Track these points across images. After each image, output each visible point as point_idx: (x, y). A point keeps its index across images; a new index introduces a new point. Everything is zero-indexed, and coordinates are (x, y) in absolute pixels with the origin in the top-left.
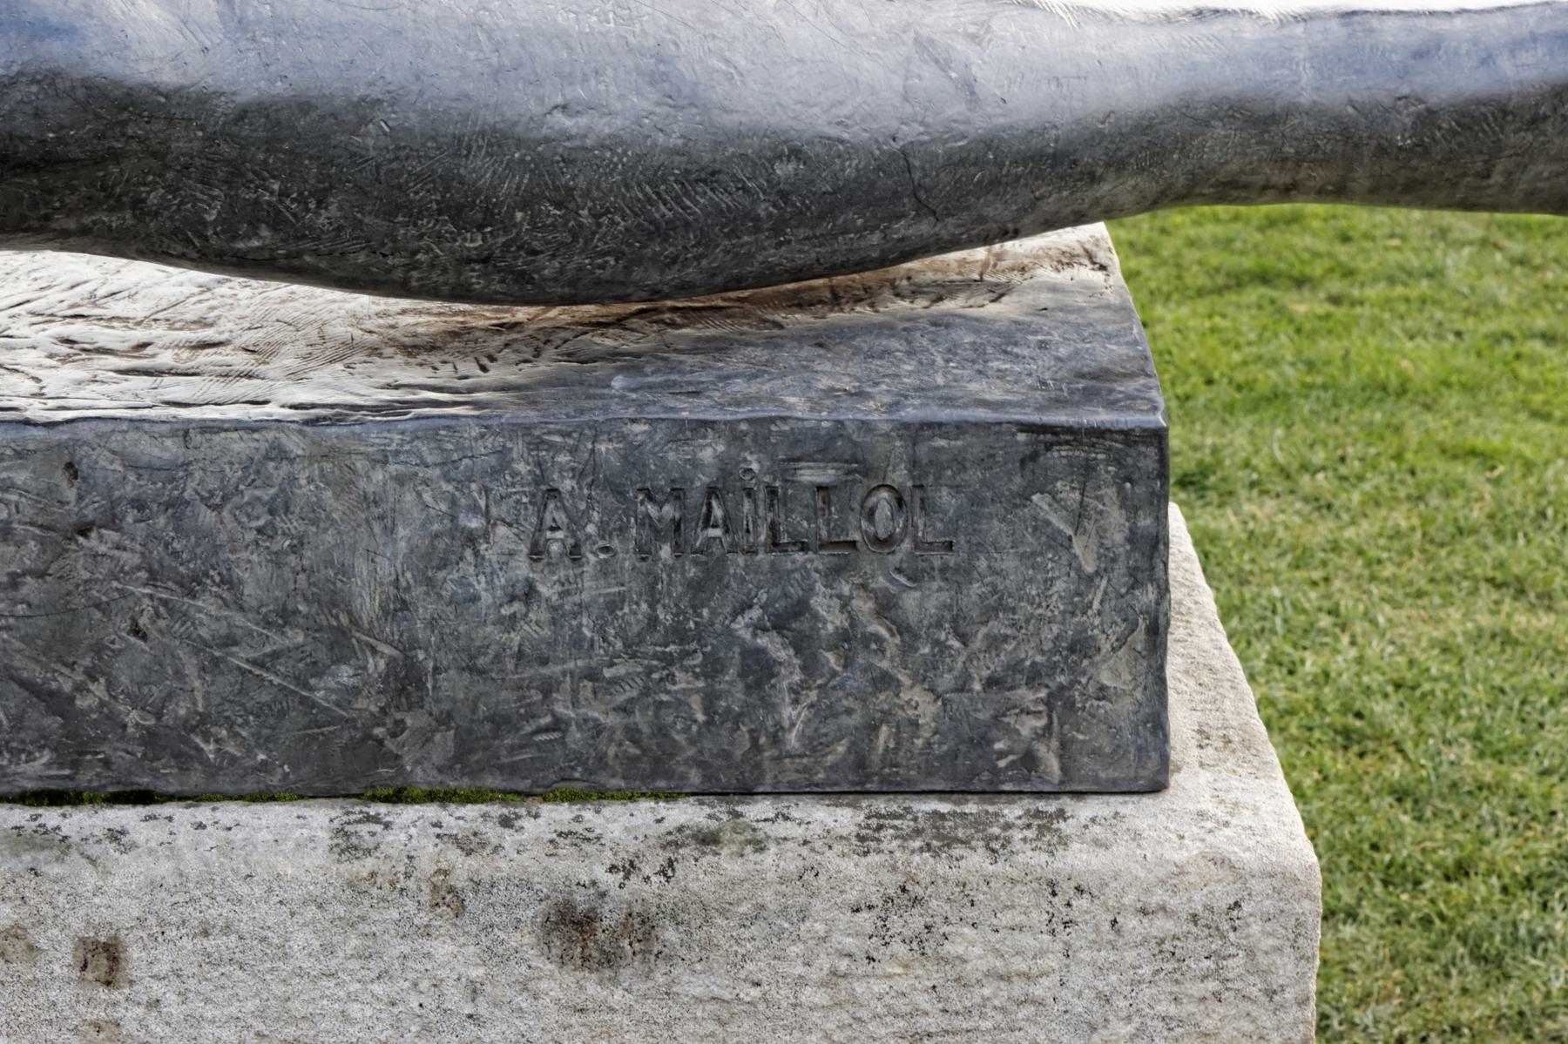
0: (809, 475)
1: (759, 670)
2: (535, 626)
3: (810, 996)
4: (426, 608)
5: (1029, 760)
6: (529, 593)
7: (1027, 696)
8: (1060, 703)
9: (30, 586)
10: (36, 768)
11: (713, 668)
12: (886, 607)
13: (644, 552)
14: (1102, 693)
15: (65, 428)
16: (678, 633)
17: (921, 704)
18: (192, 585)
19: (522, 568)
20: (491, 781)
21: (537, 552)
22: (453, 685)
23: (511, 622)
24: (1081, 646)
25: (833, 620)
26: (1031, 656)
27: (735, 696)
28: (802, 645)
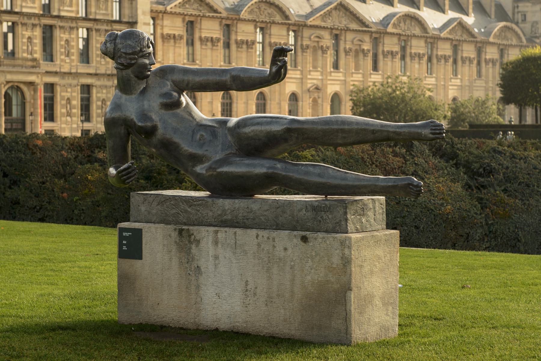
0: (323, 206)
1: (320, 221)
2: (306, 217)
3: (318, 246)
4: (299, 215)
5: (338, 230)
6: (305, 214)
7: (337, 225)
8: (340, 225)
9: (275, 213)
10: (274, 227)
11: (317, 221)
12: (328, 217)
13: (312, 211)
14: (342, 225)
15: (369, 232)
16: (315, 218)
17: (330, 225)
18: (284, 213)
19: (305, 212)
20: (303, 230)
21: (306, 211)
22: (300, 222)
23: (304, 217)
24: (341, 221)
25: (325, 218)
26: (337, 221)
27: (318, 223)
28: (323, 219)
